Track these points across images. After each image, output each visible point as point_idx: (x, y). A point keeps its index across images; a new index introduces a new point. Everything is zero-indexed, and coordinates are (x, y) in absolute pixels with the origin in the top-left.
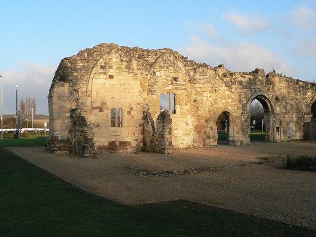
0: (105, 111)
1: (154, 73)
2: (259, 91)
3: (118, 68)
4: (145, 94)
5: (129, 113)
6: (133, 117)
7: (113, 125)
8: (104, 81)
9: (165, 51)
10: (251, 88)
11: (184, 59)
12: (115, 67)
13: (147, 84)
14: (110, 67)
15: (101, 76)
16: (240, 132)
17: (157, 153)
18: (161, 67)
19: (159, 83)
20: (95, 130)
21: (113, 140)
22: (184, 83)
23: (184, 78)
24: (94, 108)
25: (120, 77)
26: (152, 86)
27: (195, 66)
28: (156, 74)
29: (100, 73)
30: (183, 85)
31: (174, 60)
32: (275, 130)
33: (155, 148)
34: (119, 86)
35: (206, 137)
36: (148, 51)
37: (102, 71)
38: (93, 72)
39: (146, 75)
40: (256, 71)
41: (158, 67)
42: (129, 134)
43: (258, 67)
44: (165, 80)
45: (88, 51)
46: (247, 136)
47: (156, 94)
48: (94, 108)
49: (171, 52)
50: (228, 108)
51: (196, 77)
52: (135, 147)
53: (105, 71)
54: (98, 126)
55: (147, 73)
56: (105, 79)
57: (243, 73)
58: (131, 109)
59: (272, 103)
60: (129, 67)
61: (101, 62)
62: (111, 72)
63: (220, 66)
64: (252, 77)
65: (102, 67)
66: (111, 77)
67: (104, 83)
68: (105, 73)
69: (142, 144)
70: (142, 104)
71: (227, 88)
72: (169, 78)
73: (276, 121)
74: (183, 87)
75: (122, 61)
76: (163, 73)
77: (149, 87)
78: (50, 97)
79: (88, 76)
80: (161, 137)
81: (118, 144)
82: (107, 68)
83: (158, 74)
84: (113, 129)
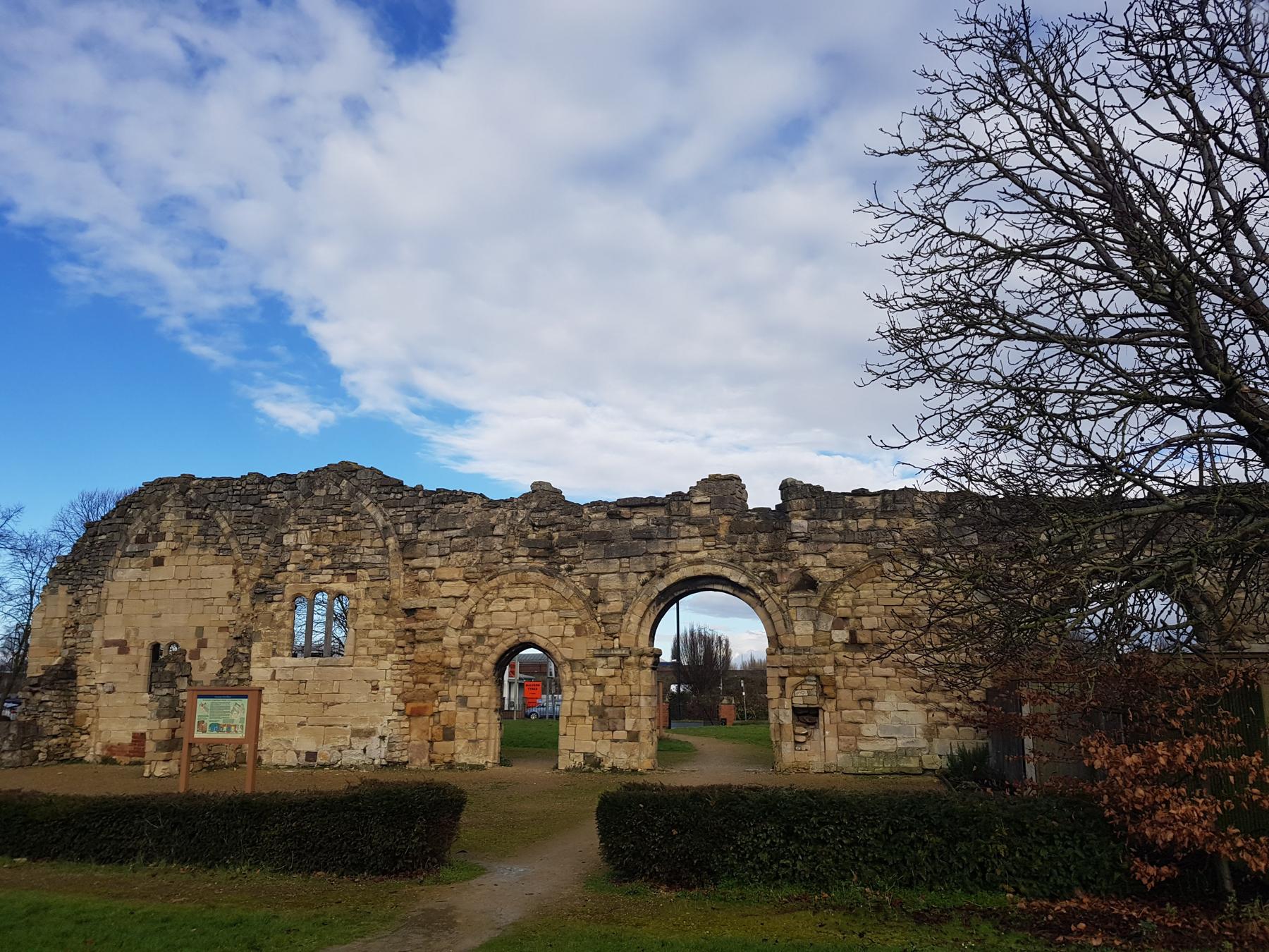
0: (133, 652)
1: (278, 540)
2: (691, 563)
3: (178, 536)
4: (246, 601)
10: (647, 553)
12: (169, 536)
13: (255, 571)
14: (160, 537)
15: (135, 562)
16: (589, 720)
18: (303, 521)
19: (290, 567)
21: (141, 728)
23: (378, 543)
24: (108, 644)
25: (180, 560)
26: (272, 578)
27: (423, 501)
28: (285, 542)
29: (133, 555)
30: (373, 566)
31: (352, 495)
35: (437, 730)
38: (119, 553)
39: (257, 547)
47: (276, 598)
48: (108, 644)
50: (535, 629)
51: (421, 536)
53: (145, 547)
55: (257, 541)
56: (144, 568)
60: (208, 535)
61: (138, 527)
62: (161, 548)
66: (159, 562)
67: (140, 580)
72: (323, 550)
75: (189, 516)
76: (304, 536)
83: (289, 540)
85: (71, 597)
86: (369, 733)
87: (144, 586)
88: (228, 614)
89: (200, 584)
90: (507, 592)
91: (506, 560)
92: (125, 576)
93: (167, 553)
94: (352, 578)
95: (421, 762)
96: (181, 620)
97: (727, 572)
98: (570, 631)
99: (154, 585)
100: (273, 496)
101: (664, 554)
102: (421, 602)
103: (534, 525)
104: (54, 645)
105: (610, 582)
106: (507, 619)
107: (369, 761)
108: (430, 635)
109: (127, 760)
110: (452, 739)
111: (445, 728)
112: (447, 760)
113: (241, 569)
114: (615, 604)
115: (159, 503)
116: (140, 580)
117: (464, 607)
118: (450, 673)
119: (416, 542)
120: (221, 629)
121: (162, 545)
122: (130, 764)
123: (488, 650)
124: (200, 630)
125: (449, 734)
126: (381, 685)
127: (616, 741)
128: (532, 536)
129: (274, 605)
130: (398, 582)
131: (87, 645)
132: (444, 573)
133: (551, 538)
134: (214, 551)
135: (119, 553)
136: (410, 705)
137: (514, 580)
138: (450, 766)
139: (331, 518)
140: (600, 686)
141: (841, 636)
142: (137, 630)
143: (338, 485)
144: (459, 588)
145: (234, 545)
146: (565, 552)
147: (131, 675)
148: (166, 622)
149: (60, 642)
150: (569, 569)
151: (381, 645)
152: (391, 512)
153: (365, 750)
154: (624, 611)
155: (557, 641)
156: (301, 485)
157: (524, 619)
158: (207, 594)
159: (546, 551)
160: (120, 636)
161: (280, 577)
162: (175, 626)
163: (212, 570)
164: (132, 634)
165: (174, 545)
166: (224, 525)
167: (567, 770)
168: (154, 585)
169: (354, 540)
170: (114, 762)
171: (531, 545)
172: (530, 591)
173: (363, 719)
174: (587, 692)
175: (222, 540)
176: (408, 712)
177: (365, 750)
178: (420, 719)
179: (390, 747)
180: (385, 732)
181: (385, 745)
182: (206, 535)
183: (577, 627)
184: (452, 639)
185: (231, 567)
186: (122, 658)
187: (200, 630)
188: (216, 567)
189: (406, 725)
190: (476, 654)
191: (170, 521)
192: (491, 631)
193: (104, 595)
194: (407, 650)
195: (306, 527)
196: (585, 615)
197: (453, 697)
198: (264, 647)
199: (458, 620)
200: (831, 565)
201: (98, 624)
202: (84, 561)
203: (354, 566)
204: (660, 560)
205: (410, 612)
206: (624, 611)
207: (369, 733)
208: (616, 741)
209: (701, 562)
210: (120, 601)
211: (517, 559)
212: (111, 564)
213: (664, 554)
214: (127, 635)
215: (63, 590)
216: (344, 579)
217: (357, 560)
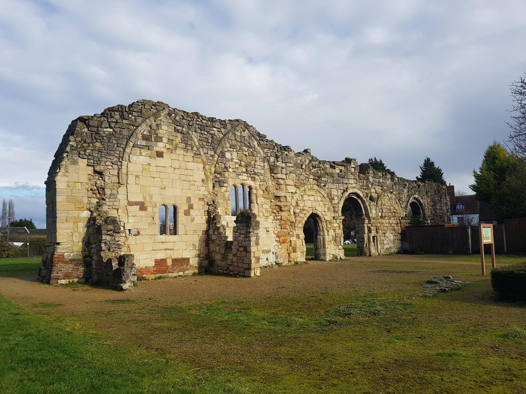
0: (150, 209)
1: (222, 155)
3: (170, 141)
4: (211, 185)
5: (187, 213)
6: (193, 220)
7: (163, 231)
8: (148, 160)
9: (236, 123)
10: (343, 183)
11: (261, 137)
12: (165, 140)
13: (213, 169)
14: (159, 139)
15: (144, 152)
16: (332, 242)
17: (235, 276)
20: (132, 240)
21: (160, 256)
22: (262, 172)
23: (262, 164)
24: (130, 204)
25: (173, 156)
27: (276, 148)
28: (226, 156)
29: (141, 147)
30: (261, 174)
31: (249, 137)
32: (372, 240)
33: (231, 268)
34: (171, 170)
35: (291, 248)
36: (212, 120)
37: (144, 143)
38: (131, 144)
39: (212, 156)
40: (348, 161)
41: (228, 145)
42: (186, 245)
43: (348, 157)
44: (237, 166)
45: (120, 109)
46: (340, 247)
47: (225, 185)
48: (130, 204)
49: (247, 126)
50: (317, 208)
51: (279, 164)
52: (195, 267)
53: (149, 143)
54: (139, 233)
56: (151, 157)
57: (334, 162)
58: (191, 207)
59: (367, 204)
61: (144, 129)
62: (160, 146)
63: (306, 151)
64: (343, 168)
65: (145, 138)
66: (160, 155)
67: (149, 164)
68: (149, 148)
69: (206, 262)
70: (206, 200)
71: (315, 182)
73: (372, 228)
74: (262, 177)
76: (235, 154)
77: (216, 174)
78: (51, 184)
79: (121, 150)
80: (242, 249)
81: (169, 263)
82: (153, 139)
83: (228, 155)
84: (164, 236)
85: (91, 168)
86: (268, 252)
87: (152, 169)
88: (203, 191)
89: (187, 172)
90: (308, 193)
91: (307, 180)
92: (137, 161)
93: (164, 150)
94: (253, 179)
95: (286, 263)
96: (178, 192)
97: (359, 192)
98: (326, 210)
99: (159, 169)
100: (215, 129)
101: (346, 184)
102: (282, 194)
103: (313, 166)
104: (81, 202)
105: (334, 192)
106: (308, 204)
107: (270, 264)
108: (287, 208)
109: (153, 276)
110: (296, 252)
111: (293, 248)
112: (295, 260)
113: (207, 167)
114: (336, 201)
115: (156, 116)
116: (149, 164)
117: (296, 197)
118: (293, 224)
119: (277, 166)
120: (200, 199)
121: (160, 144)
122: (155, 279)
123: (303, 216)
124: (189, 199)
125: (295, 251)
126: (270, 230)
127: (339, 249)
128: (312, 171)
129: (224, 189)
130: (271, 184)
131: (115, 203)
132: (289, 182)
133: (318, 173)
134: (192, 154)
135: (131, 144)
136: (281, 239)
137: (309, 188)
138: (296, 263)
139: (245, 148)
140: (335, 230)
141: (380, 214)
142: (151, 196)
143: (244, 131)
144: (292, 189)
145: (202, 153)
146: (323, 179)
147: (150, 224)
148: (169, 192)
149: (85, 200)
150: (325, 186)
151: (267, 211)
152: (266, 150)
153: (267, 259)
154: (338, 203)
155: (323, 213)
156: (229, 127)
157: (314, 204)
158: (191, 179)
159: (318, 178)
160: (140, 199)
161: (227, 174)
162: (175, 195)
163: (191, 165)
164: (148, 199)
165: (168, 146)
166: (196, 140)
167: (330, 260)
168: (159, 169)
169: (252, 161)
170: (144, 279)
171: (314, 174)
172: (313, 193)
173: (265, 245)
174: (332, 232)
175: (195, 148)
176: (281, 241)
177: (267, 259)
178: (284, 244)
179: (277, 257)
180: (274, 251)
181: (274, 256)
182: (186, 144)
183: (328, 208)
184: (292, 211)
185: (202, 165)
186: (143, 213)
187: (189, 199)
188: (195, 164)
189: (280, 247)
190: (301, 217)
191: (165, 130)
192: (305, 208)
193: (124, 170)
194: (277, 214)
195: (235, 150)
196: (330, 204)
197: (295, 235)
198: (222, 210)
199: (294, 204)
200: (376, 193)
201: (122, 190)
202: (98, 144)
203: (255, 174)
204: (346, 186)
205: (277, 197)
206: (338, 203)
207: (268, 252)
208: (339, 249)
209: (354, 188)
210: (137, 176)
211: (310, 180)
212: (128, 150)
213: (346, 184)
214: (144, 198)
215: (82, 163)
216: (250, 178)
217: (256, 171)
